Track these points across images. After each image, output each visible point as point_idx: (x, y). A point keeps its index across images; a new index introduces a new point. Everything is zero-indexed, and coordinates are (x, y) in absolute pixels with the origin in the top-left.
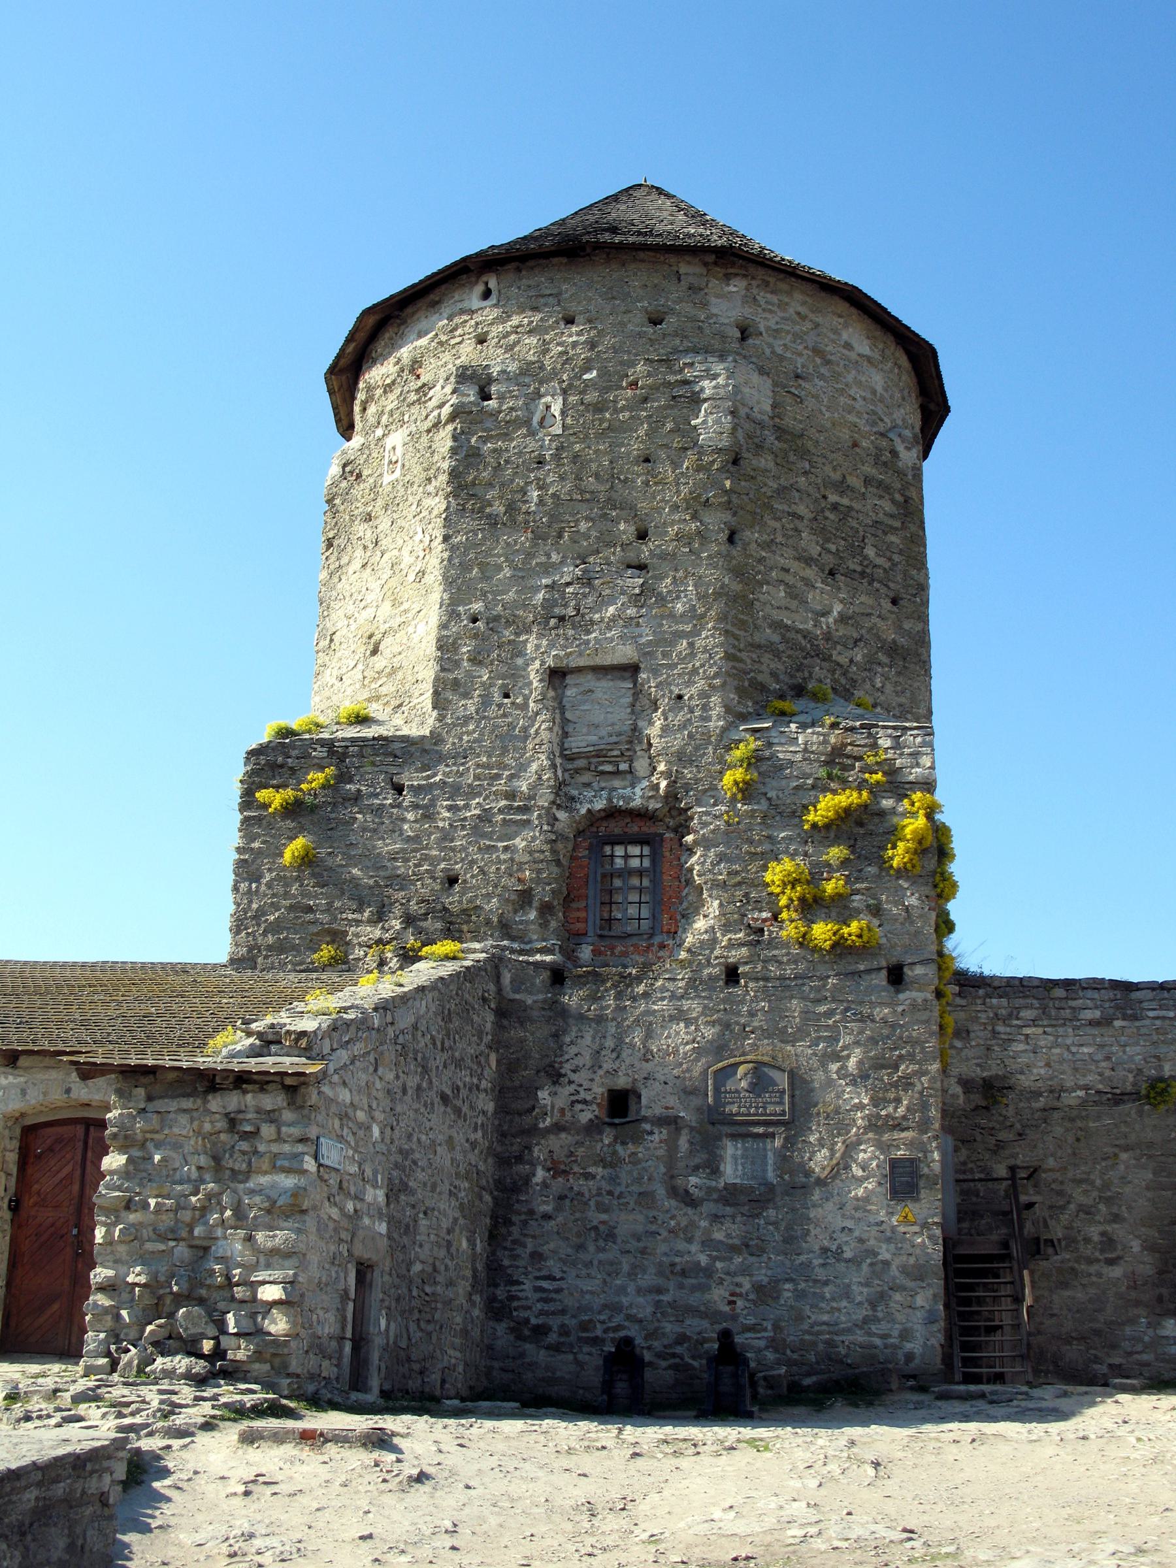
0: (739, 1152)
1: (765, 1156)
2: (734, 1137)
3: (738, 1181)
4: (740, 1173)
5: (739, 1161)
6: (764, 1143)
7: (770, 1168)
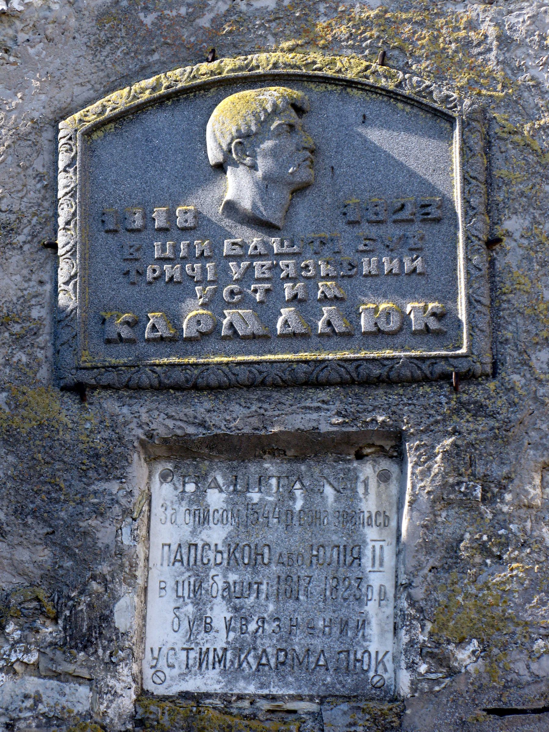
0: (216, 534)
1: (353, 554)
2: (185, 453)
3: (209, 682)
4: (219, 640)
5: (217, 581)
6: (347, 489)
7: (377, 614)
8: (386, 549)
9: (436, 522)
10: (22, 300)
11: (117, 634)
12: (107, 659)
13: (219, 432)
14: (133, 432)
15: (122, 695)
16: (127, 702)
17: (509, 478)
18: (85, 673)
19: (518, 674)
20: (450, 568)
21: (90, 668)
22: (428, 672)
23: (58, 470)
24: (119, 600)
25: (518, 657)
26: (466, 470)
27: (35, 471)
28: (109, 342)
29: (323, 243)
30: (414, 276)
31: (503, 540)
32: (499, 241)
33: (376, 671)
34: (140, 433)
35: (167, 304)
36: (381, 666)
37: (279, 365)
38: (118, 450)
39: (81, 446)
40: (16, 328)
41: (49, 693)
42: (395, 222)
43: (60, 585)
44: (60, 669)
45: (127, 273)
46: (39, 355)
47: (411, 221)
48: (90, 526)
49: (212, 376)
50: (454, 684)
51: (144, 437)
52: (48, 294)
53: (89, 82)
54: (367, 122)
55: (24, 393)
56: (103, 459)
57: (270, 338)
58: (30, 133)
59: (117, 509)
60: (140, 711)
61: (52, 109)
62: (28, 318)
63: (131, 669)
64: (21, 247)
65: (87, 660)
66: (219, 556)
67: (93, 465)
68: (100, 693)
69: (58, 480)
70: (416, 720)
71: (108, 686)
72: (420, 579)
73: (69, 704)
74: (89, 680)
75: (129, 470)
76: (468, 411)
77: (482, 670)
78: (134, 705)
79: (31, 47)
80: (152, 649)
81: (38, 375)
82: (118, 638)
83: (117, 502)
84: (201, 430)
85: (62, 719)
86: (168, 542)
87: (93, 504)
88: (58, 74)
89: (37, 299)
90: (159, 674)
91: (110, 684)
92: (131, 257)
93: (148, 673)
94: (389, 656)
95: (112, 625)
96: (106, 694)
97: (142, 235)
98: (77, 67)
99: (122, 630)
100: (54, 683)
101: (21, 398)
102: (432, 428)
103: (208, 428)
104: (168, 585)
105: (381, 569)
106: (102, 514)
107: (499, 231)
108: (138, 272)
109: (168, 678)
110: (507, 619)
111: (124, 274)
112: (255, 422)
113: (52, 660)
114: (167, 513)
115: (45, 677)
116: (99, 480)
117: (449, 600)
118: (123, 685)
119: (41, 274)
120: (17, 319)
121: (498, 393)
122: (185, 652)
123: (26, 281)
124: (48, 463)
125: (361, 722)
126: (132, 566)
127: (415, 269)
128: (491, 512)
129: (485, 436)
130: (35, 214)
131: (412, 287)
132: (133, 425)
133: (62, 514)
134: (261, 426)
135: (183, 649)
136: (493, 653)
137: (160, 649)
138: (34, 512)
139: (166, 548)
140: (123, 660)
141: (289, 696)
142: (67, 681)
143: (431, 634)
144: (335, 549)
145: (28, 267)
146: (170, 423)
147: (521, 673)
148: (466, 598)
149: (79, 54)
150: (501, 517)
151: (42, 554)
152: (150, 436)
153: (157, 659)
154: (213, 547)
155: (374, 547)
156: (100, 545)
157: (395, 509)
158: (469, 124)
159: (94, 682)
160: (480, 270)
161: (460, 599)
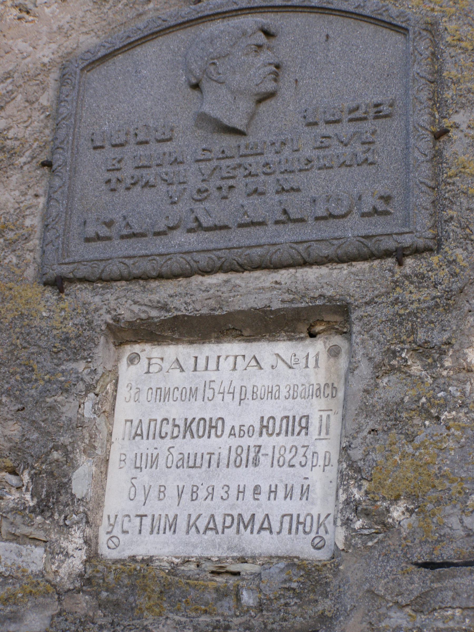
8: (332, 417)
9: (377, 386)
10: (18, 211)
11: (72, 500)
12: (61, 523)
13: (180, 313)
14: (102, 318)
15: (73, 556)
16: (76, 562)
17: (449, 343)
18: (41, 535)
19: (451, 528)
20: (389, 429)
21: (46, 530)
22: (363, 528)
23: (33, 353)
24: (78, 467)
25: (451, 511)
26: (408, 337)
27: (13, 355)
28: (88, 240)
29: (283, 143)
30: (365, 166)
31: (442, 402)
32: (445, 132)
33: (317, 533)
34: (108, 318)
35: (141, 205)
36: (322, 528)
37: (236, 250)
38: (87, 333)
39: (55, 332)
40: (11, 235)
41: (7, 554)
42: (351, 120)
43: (26, 456)
44: (18, 532)
45: (109, 181)
46: (28, 257)
47: (365, 119)
48: (56, 401)
49: (175, 264)
50: (387, 539)
51: (111, 322)
52: (41, 206)
53: (92, 30)
54: (330, 40)
55: (11, 289)
56: (73, 342)
57: (230, 228)
58: (39, 74)
59: (81, 386)
60: (89, 571)
61: (60, 54)
62: (22, 226)
63: (84, 531)
64: (22, 167)
65: (44, 523)
66: (176, 429)
67: (64, 348)
68: (52, 553)
69: (32, 362)
70: (349, 574)
71: (61, 547)
72: (359, 440)
73: (24, 564)
74: (44, 542)
75: (96, 351)
76: (412, 283)
77: (416, 525)
78: (85, 565)
79: (48, 7)
80: (109, 517)
81: (25, 274)
82: (73, 503)
83: (82, 379)
84: (163, 313)
85: (17, 578)
86: (130, 418)
87: (61, 382)
88: (67, 26)
89: (31, 210)
90: (114, 540)
91: (63, 545)
92: (113, 167)
93: (103, 538)
94: (331, 518)
95: (69, 491)
96: (58, 554)
97: (125, 149)
98: (84, 19)
99: (78, 496)
100: (13, 545)
101: (7, 293)
102: (376, 299)
103: (168, 311)
104: (128, 457)
105: (326, 437)
106: (67, 391)
107: (446, 123)
108: (118, 180)
109: (122, 543)
110: (442, 476)
111: (106, 183)
112: (212, 303)
113: (12, 523)
114: (131, 391)
115: (6, 540)
116: (67, 361)
117: (387, 460)
118: (75, 546)
119: (36, 189)
120: (11, 227)
121: (441, 266)
122: (139, 519)
123: (23, 196)
124: (25, 348)
125: (295, 579)
126: (91, 438)
127: (367, 159)
128: (432, 377)
129: (426, 305)
130: (36, 140)
131: (363, 176)
132: (103, 311)
133: (33, 392)
134: (218, 307)
135: (137, 516)
136: (427, 508)
137: (116, 516)
138: (8, 390)
139: (128, 423)
140: (78, 523)
141: (233, 558)
142: (25, 544)
143: (367, 493)
144: (285, 421)
145: (26, 183)
146: (136, 308)
147: (455, 527)
148: (403, 456)
149: (86, 9)
150: (442, 381)
151: (13, 429)
152: (116, 319)
153: (113, 526)
154: (171, 421)
155: (321, 416)
156: (63, 418)
157: (342, 381)
158: (420, 33)
159: (48, 544)
160: (426, 155)
161: (397, 458)
